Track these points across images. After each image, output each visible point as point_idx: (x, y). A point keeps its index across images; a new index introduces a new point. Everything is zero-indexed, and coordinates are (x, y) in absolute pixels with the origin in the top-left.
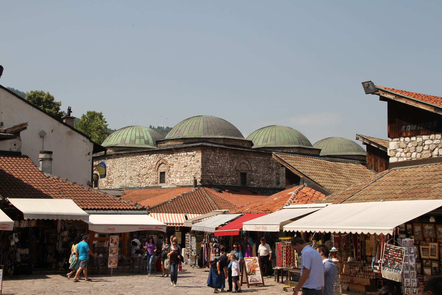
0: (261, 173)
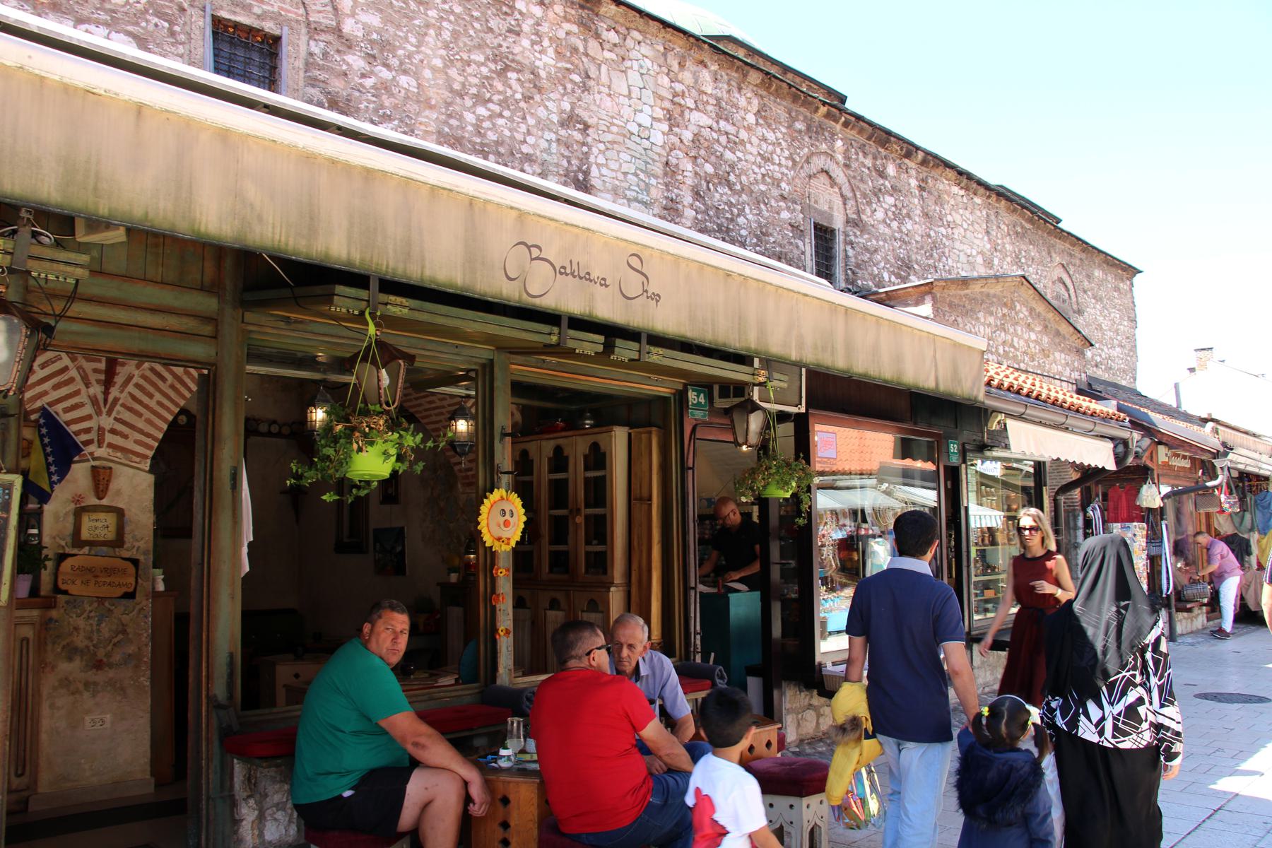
0: (427, 73)
